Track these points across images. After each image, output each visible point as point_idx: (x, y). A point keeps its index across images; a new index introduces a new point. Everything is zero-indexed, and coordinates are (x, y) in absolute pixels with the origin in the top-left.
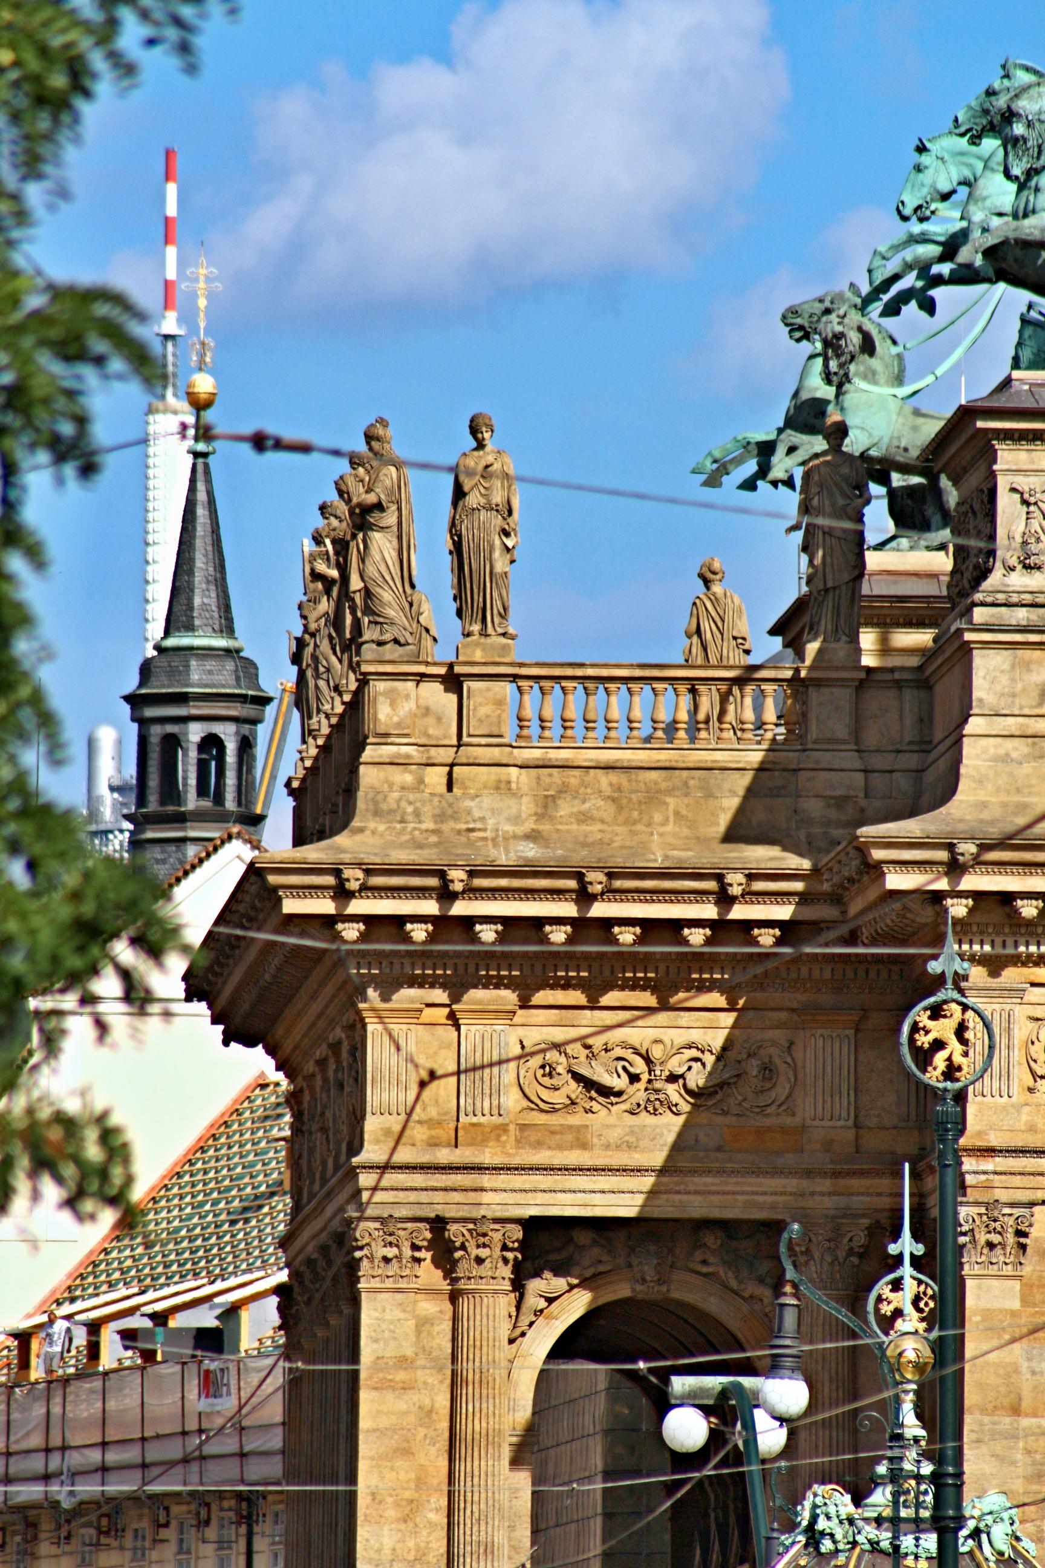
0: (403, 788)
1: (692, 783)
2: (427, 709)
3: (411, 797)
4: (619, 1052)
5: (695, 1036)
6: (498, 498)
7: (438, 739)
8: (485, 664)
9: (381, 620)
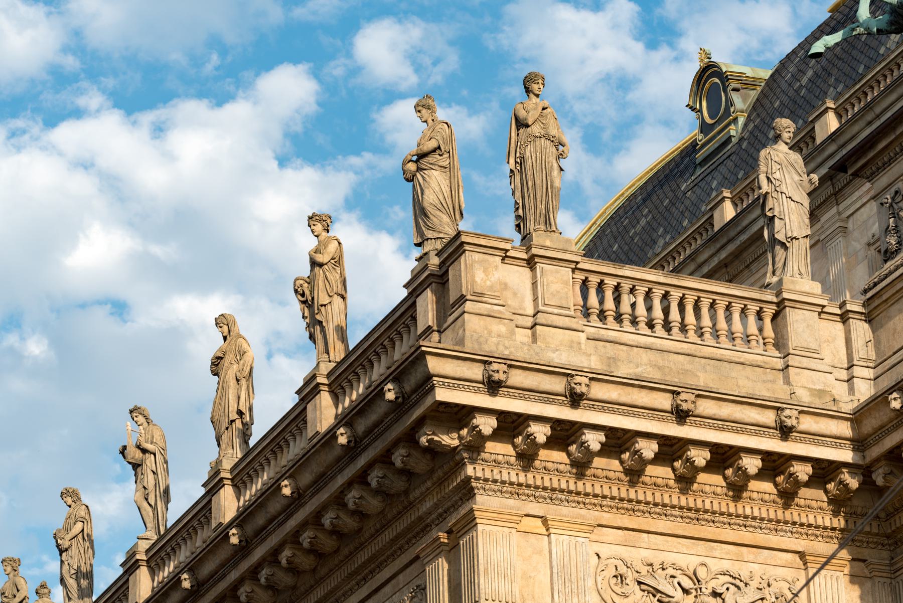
0: (499, 336)
1: (708, 368)
2: (506, 284)
3: (507, 344)
4: (671, 571)
5: (726, 565)
7: (515, 309)
8: (556, 250)
9: (441, 235)
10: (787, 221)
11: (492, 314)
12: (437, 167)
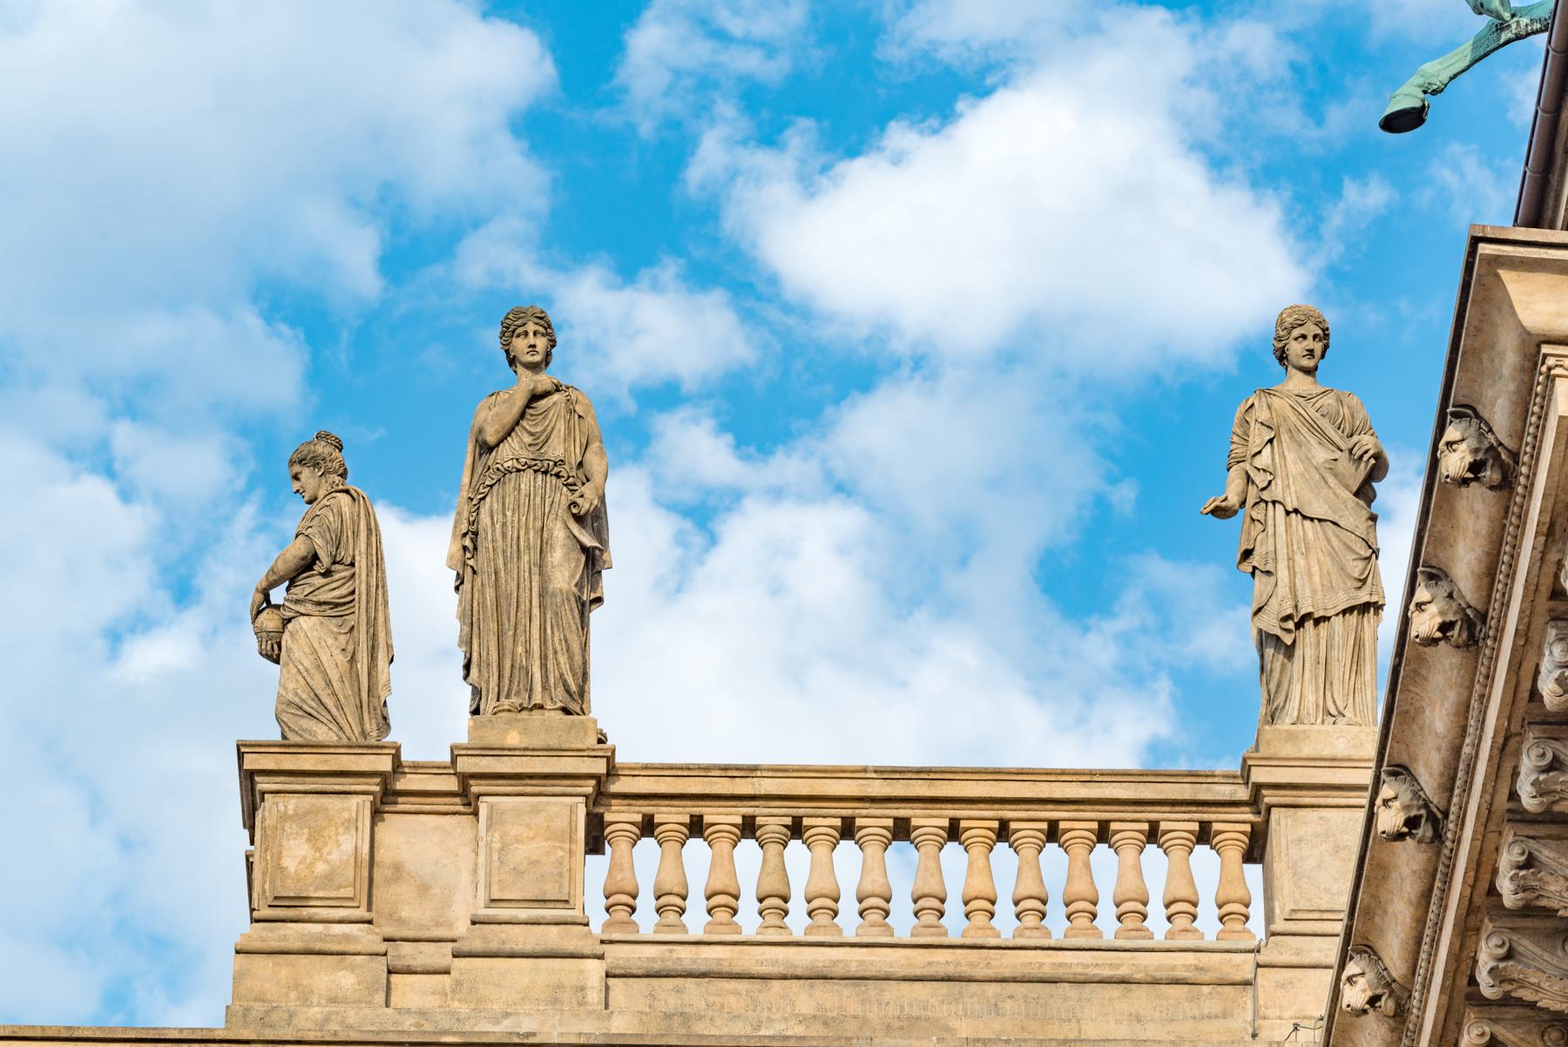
0: (333, 1000)
6: (555, 450)
8: (525, 751)
10: (1283, 573)
11: (318, 946)
12: (309, 608)
